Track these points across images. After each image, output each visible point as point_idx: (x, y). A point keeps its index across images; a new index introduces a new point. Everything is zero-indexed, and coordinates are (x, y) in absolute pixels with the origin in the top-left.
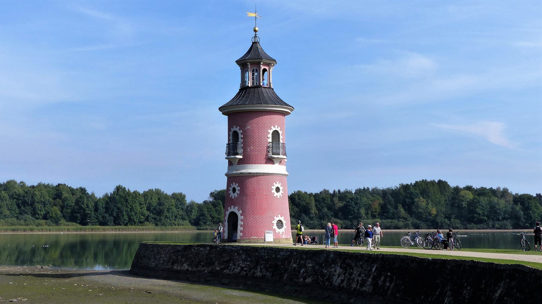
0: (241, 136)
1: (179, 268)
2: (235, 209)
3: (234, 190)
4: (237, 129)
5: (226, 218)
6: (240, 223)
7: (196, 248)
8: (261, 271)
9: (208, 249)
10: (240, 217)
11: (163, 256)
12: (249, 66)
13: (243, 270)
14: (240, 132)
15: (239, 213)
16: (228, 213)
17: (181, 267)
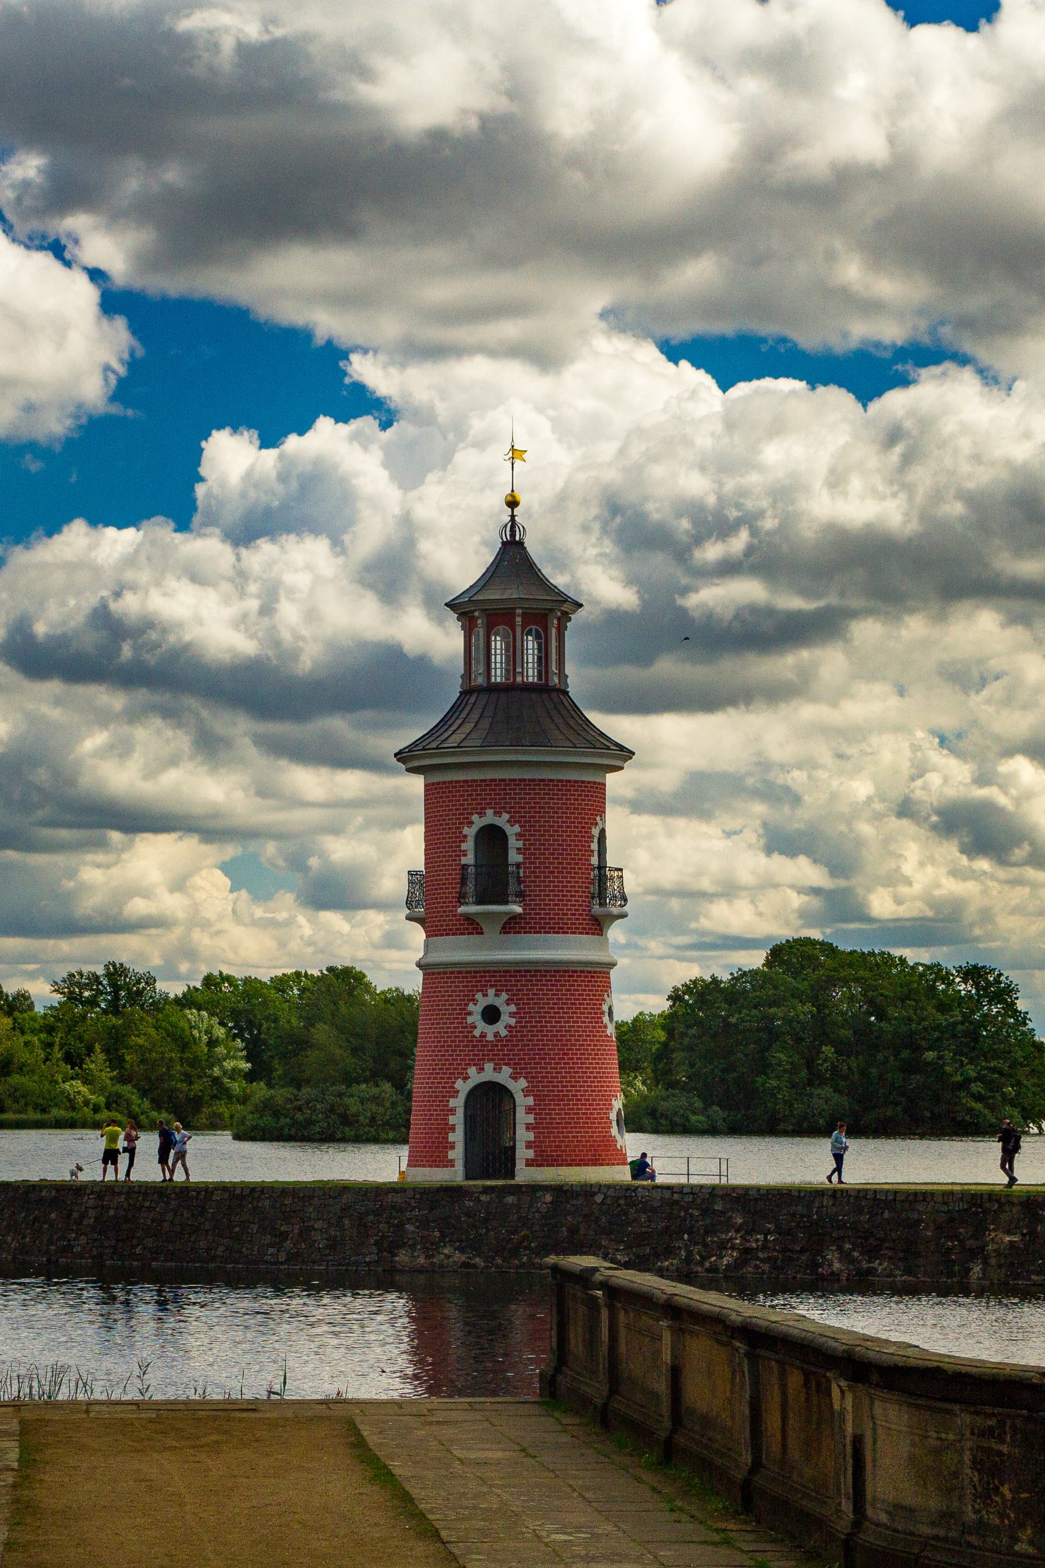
0: (514, 843)
1: (422, 1260)
2: (504, 1076)
3: (491, 1015)
4: (502, 821)
5: (458, 1103)
6: (523, 1118)
7: (483, 1198)
8: (846, 1257)
9: (548, 1198)
10: (523, 1102)
11: (319, 1225)
12: (519, 619)
13: (758, 1259)
14: (513, 831)
15: (517, 1086)
16: (463, 1087)
17: (427, 1257)
